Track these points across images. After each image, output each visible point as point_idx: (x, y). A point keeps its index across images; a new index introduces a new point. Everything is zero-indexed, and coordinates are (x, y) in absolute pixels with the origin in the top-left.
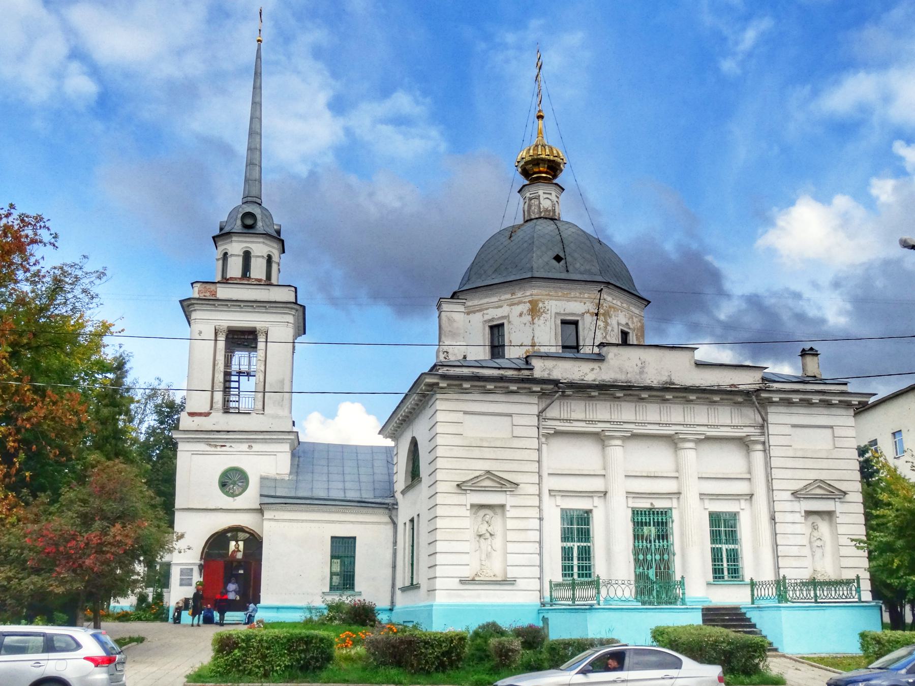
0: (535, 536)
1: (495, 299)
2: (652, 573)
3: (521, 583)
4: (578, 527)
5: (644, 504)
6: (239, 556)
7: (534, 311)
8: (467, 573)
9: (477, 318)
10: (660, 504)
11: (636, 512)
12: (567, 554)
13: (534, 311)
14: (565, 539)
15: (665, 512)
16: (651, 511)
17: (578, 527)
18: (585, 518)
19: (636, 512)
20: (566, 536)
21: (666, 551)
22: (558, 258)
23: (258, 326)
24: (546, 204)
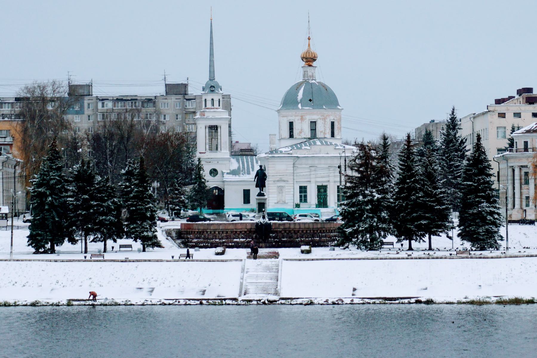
0: (292, 193)
1: (290, 113)
2: (322, 201)
3: (289, 204)
4: (303, 190)
5: (320, 184)
6: (217, 194)
7: (302, 119)
8: (276, 201)
9: (285, 119)
10: (324, 184)
11: (318, 186)
12: (301, 196)
13: (302, 119)
14: (300, 193)
15: (326, 186)
16: (322, 186)
17: (303, 190)
18: (305, 188)
19: (318, 186)
20: (300, 192)
21: (326, 196)
22: (310, 100)
23: (218, 124)
24: (310, 74)
